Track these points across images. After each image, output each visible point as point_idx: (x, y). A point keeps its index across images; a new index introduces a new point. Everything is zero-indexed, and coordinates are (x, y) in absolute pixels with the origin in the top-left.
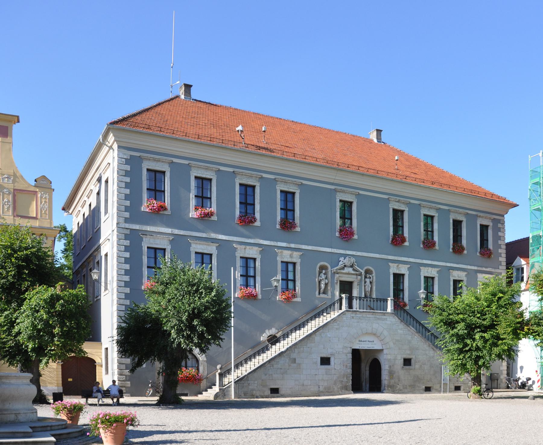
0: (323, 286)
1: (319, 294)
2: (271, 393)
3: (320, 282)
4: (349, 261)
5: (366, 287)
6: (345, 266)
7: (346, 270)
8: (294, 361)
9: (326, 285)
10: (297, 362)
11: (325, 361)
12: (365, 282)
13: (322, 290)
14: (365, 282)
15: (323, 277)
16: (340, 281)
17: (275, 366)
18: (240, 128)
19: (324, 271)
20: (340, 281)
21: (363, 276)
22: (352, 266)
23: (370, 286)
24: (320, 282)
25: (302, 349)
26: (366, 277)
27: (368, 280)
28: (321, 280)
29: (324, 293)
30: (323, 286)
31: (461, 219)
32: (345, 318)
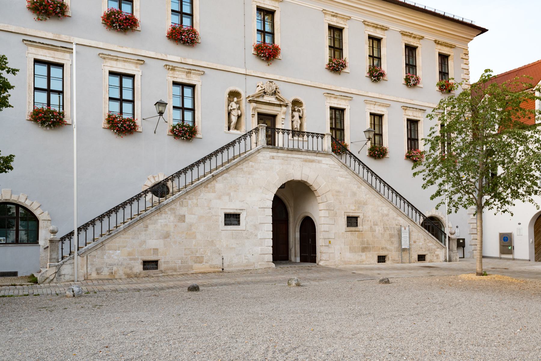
0: (234, 119)
1: (229, 129)
2: (144, 269)
3: (229, 114)
4: (270, 86)
5: (294, 123)
6: (265, 93)
8: (182, 218)
9: (239, 117)
10: (187, 220)
11: (232, 219)
12: (293, 117)
13: (233, 124)
14: (293, 117)
15: (234, 105)
16: (259, 114)
17: (151, 227)
19: (235, 99)
20: (259, 114)
22: (275, 93)
24: (229, 114)
25: (195, 201)
26: (293, 111)
27: (296, 114)
28: (231, 110)
29: (236, 128)
30: (234, 119)
31: (415, 45)
32: (261, 158)
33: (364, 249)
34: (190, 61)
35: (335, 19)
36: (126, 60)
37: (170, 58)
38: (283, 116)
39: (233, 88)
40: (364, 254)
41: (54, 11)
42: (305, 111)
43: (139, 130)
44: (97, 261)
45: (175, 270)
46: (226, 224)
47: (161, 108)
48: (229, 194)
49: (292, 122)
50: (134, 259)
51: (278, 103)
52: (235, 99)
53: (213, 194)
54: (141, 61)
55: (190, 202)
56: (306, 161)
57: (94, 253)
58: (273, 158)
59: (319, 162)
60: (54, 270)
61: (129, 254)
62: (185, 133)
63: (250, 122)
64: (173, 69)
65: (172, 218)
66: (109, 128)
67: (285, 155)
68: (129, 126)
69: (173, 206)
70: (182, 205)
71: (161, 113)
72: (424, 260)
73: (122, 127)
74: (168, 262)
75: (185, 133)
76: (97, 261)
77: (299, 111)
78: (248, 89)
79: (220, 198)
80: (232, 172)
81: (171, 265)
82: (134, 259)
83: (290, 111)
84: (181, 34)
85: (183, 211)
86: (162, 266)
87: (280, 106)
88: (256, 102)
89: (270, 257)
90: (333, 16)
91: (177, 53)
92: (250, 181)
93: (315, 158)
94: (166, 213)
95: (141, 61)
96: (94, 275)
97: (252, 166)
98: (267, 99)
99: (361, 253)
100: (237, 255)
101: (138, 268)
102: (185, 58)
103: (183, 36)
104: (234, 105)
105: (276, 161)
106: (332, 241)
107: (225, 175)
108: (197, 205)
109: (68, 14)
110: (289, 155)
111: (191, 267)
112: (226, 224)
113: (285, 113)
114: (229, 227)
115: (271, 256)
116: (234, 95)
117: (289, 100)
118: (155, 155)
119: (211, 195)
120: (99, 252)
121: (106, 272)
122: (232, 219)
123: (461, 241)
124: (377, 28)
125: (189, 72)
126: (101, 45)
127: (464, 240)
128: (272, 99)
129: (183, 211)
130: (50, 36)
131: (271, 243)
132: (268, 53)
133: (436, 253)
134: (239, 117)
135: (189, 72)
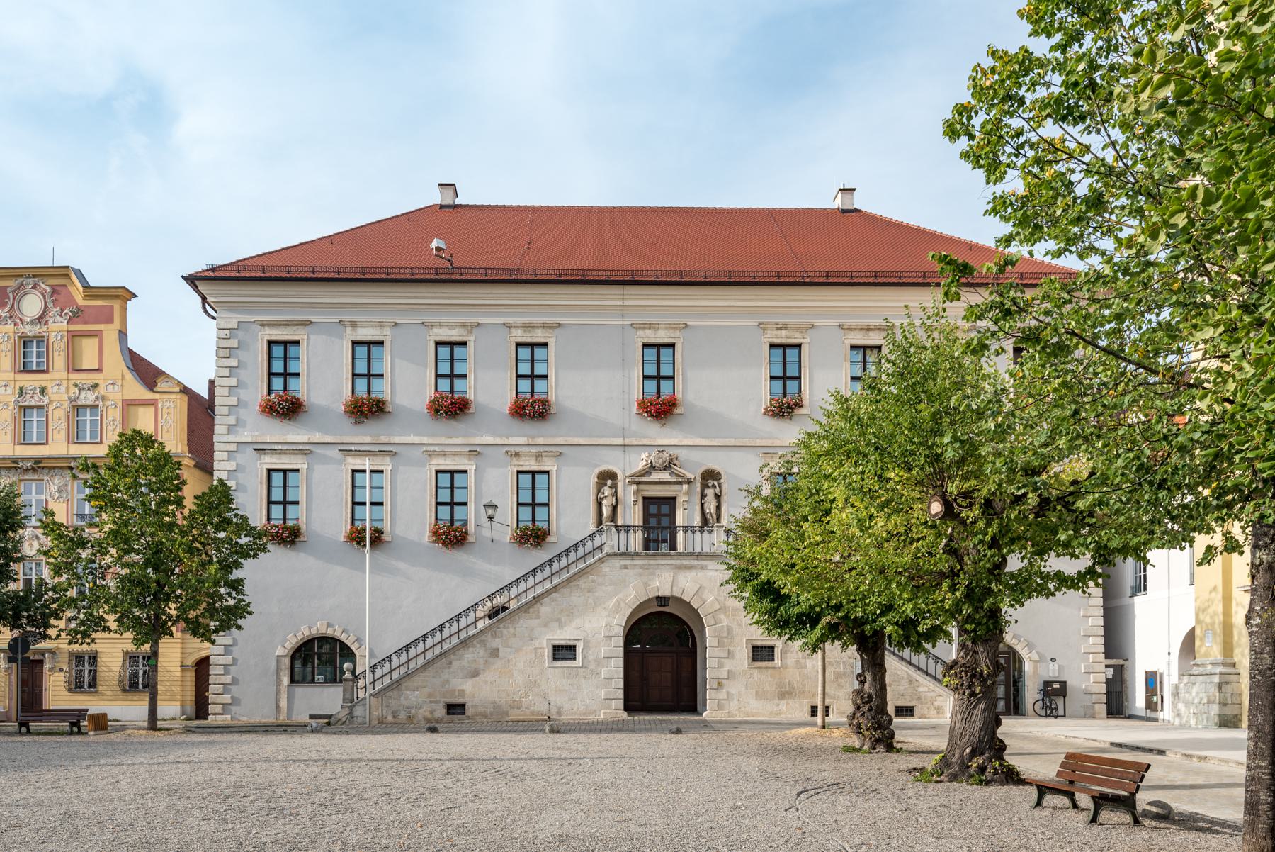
2: (448, 713)
3: (600, 504)
6: (654, 468)
7: (655, 476)
9: (615, 508)
11: (563, 652)
12: (703, 496)
14: (703, 496)
15: (607, 491)
16: (644, 498)
17: (456, 664)
18: (434, 244)
19: (609, 482)
20: (644, 498)
21: (699, 485)
22: (667, 467)
23: (714, 503)
25: (511, 630)
26: (705, 486)
27: (710, 492)
33: (782, 695)
34: (540, 441)
35: (784, 332)
36: (455, 454)
37: (513, 441)
38: (685, 498)
39: (604, 467)
40: (783, 702)
41: (370, 411)
42: (724, 486)
43: (470, 539)
44: (393, 702)
45: (485, 716)
46: (555, 659)
47: (490, 512)
48: (559, 620)
49: (702, 505)
50: (436, 702)
51: (674, 479)
52: (609, 482)
53: (537, 621)
54: (474, 452)
55: (505, 632)
56: (679, 568)
57: (390, 694)
58: (626, 567)
59: (702, 568)
60: (346, 711)
61: (430, 695)
62: (533, 536)
63: (632, 514)
64: (517, 455)
65: (482, 653)
66: (435, 542)
67: (645, 562)
68: (455, 537)
69: (483, 638)
70: (494, 636)
71: (491, 518)
72: (912, 715)
73: (452, 537)
74: (476, 706)
75: (533, 536)
76: (393, 702)
77: (714, 486)
78: (627, 465)
79: (546, 625)
80: (566, 591)
81: (480, 710)
82: (436, 702)
83: (699, 489)
84: (524, 408)
85: (496, 643)
86: (469, 711)
87: (680, 483)
88: (639, 483)
89: (621, 704)
90: (781, 329)
91: (522, 435)
92: (590, 601)
93: (696, 562)
94: (474, 646)
95: (474, 452)
96: (390, 718)
97: (593, 581)
98: (655, 476)
99: (777, 701)
100: (571, 700)
101: (441, 712)
102: (533, 437)
103: (532, 410)
104: (607, 491)
105: (630, 572)
106: (724, 682)
107: (554, 595)
108: (514, 635)
109: (387, 409)
110: (652, 562)
111: (507, 714)
112: (555, 659)
113: (688, 493)
114: (559, 664)
115: (622, 702)
116: (607, 477)
117: (694, 474)
118: (494, 567)
119: (534, 623)
120: (395, 692)
121: (403, 716)
122: (564, 652)
123: (1056, 686)
124: (868, 330)
125: (539, 456)
126: (425, 440)
127: (1063, 684)
128: (665, 476)
129: (496, 643)
130: (368, 440)
131: (621, 684)
132: (660, 409)
133: (936, 704)
134: (615, 508)
135: (539, 456)
